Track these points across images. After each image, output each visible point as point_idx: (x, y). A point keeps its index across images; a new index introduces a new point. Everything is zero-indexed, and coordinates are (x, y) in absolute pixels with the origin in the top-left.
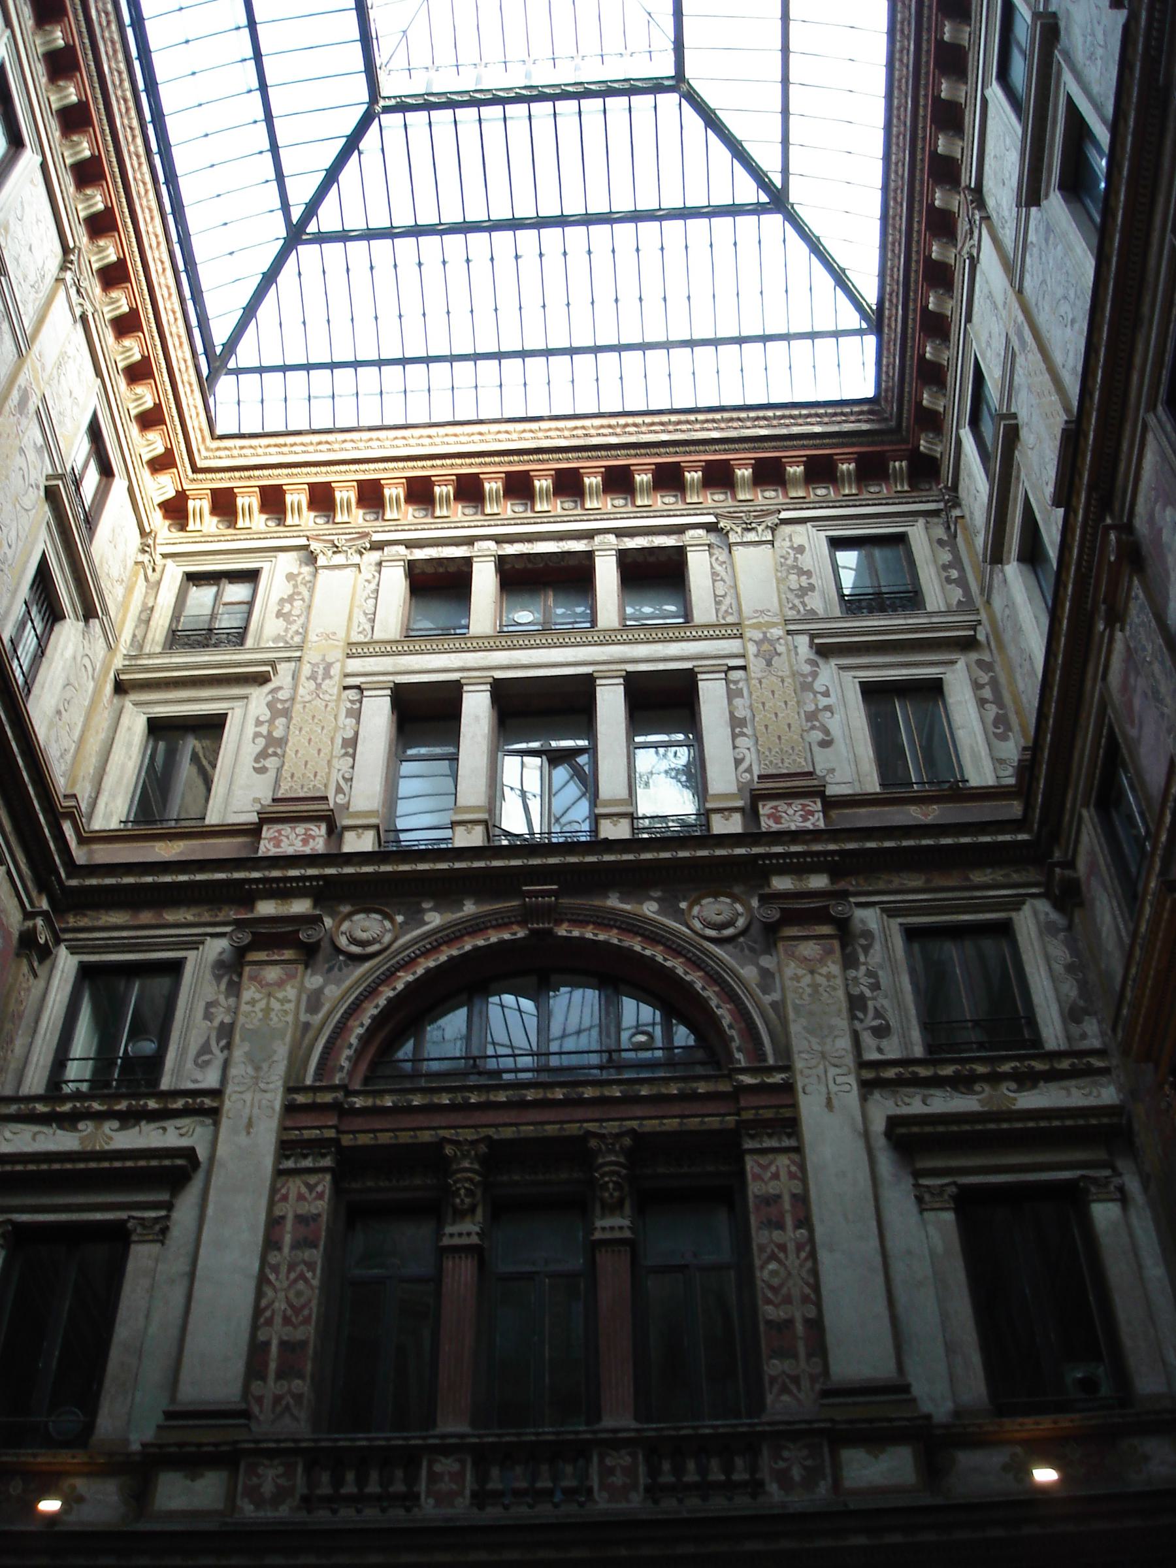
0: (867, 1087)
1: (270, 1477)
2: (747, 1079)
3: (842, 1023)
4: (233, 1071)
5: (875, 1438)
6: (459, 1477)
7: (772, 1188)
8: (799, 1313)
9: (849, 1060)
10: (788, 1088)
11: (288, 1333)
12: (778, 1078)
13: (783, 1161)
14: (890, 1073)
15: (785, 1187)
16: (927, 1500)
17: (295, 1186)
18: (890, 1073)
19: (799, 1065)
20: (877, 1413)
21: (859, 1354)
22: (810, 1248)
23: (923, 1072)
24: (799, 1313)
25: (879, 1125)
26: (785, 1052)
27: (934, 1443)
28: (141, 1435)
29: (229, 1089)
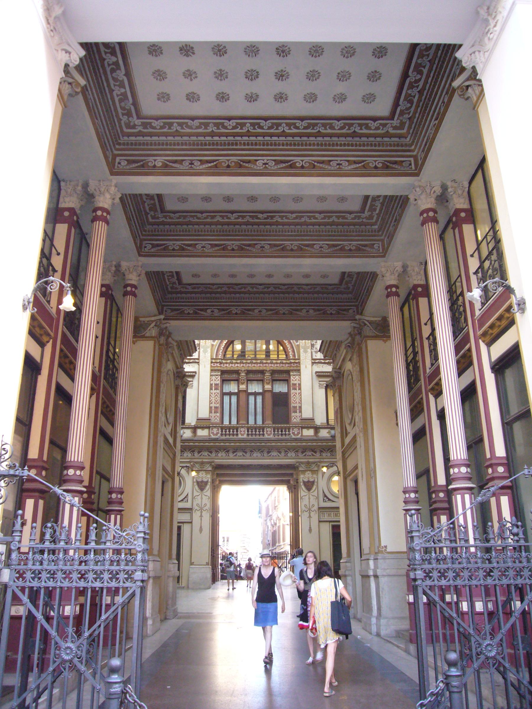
0: (313, 363)
1: (215, 431)
2: (292, 361)
3: (309, 350)
4: (201, 354)
5: (308, 428)
6: (244, 431)
7: (295, 382)
8: (298, 405)
9: (310, 358)
10: (299, 363)
11: (215, 405)
12: (297, 361)
13: (297, 377)
14: (317, 361)
15: (297, 382)
16: (315, 438)
17: (214, 377)
18: (317, 361)
19: (301, 358)
20: (308, 423)
21: (307, 413)
22: (300, 394)
23: (323, 361)
24: (298, 405)
25: (314, 372)
26: (299, 356)
27: (317, 429)
28: (193, 423)
29: (201, 358)
